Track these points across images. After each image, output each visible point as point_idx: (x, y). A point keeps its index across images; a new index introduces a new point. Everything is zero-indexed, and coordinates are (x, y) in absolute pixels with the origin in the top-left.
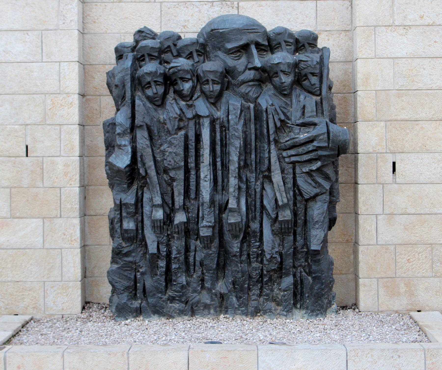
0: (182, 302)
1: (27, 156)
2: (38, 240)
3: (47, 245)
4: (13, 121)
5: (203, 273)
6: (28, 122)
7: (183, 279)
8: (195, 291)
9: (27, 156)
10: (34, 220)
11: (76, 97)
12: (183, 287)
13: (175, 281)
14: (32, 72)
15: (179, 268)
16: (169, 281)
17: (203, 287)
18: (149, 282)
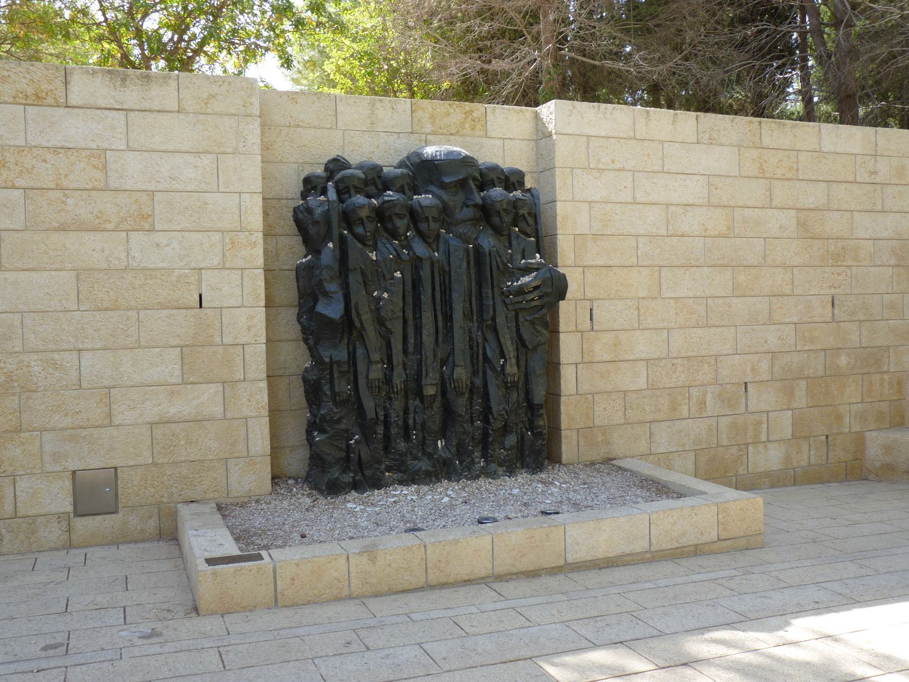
0: (401, 472)
1: (201, 306)
2: (218, 410)
3: (229, 415)
4: (183, 264)
5: (424, 438)
6: (202, 265)
7: (402, 445)
8: (416, 458)
9: (201, 306)
10: (212, 385)
11: (261, 235)
12: (401, 455)
13: (393, 448)
14: (206, 203)
15: (398, 433)
16: (386, 449)
17: (424, 453)
18: (365, 453)
